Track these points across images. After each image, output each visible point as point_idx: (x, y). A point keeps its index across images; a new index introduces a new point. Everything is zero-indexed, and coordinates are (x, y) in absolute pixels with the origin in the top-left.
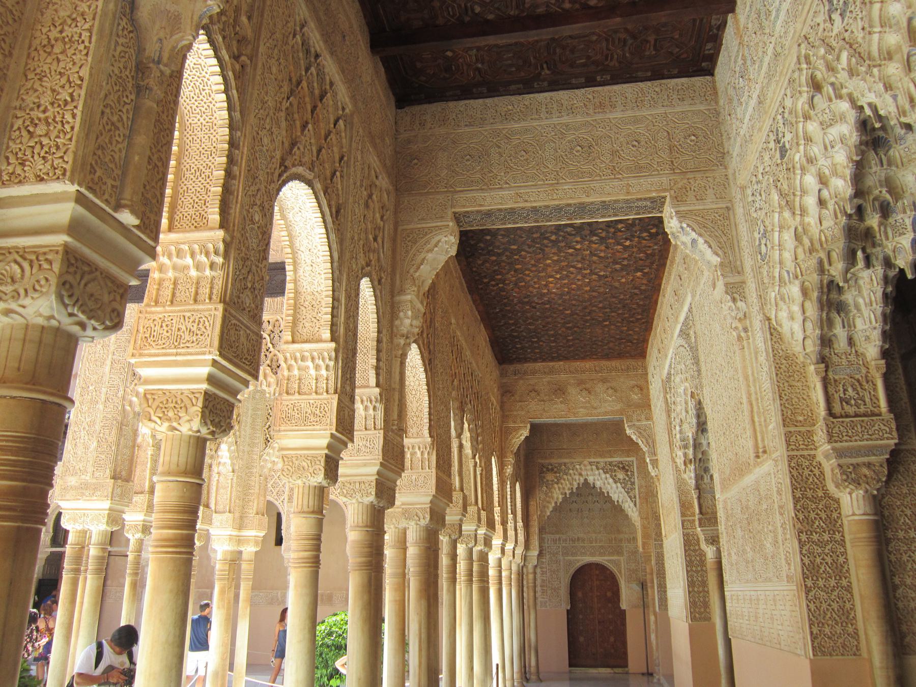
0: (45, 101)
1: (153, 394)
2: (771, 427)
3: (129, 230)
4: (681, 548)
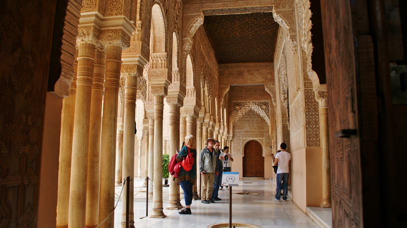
3: (131, 25)
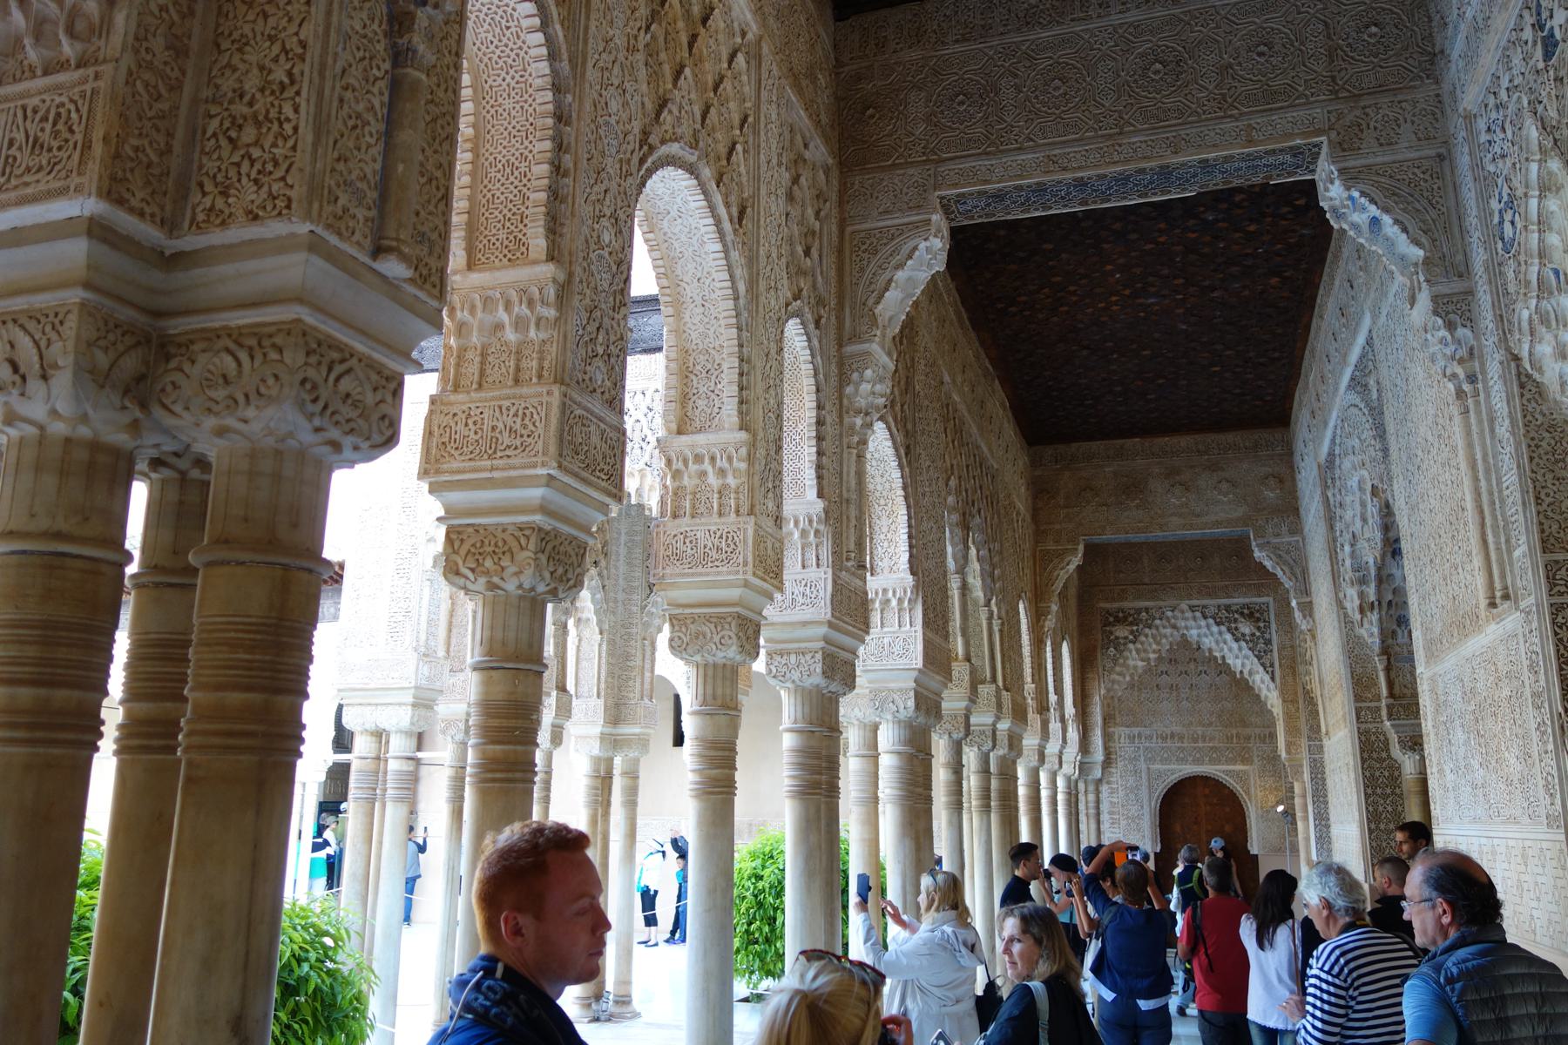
0: (252, 84)
1: (459, 533)
2: (1517, 553)
3: (397, 287)
4: (1354, 755)
